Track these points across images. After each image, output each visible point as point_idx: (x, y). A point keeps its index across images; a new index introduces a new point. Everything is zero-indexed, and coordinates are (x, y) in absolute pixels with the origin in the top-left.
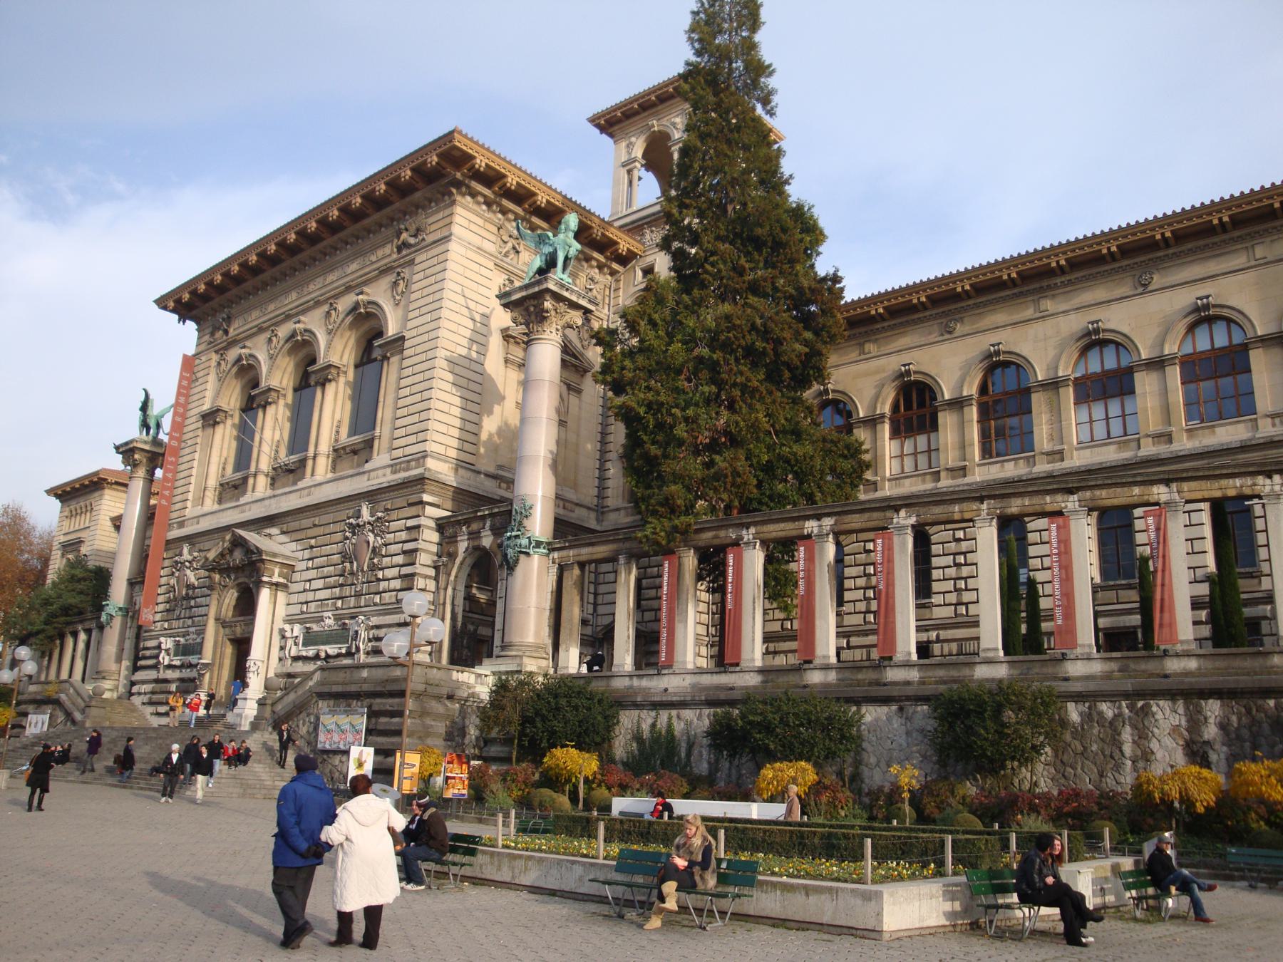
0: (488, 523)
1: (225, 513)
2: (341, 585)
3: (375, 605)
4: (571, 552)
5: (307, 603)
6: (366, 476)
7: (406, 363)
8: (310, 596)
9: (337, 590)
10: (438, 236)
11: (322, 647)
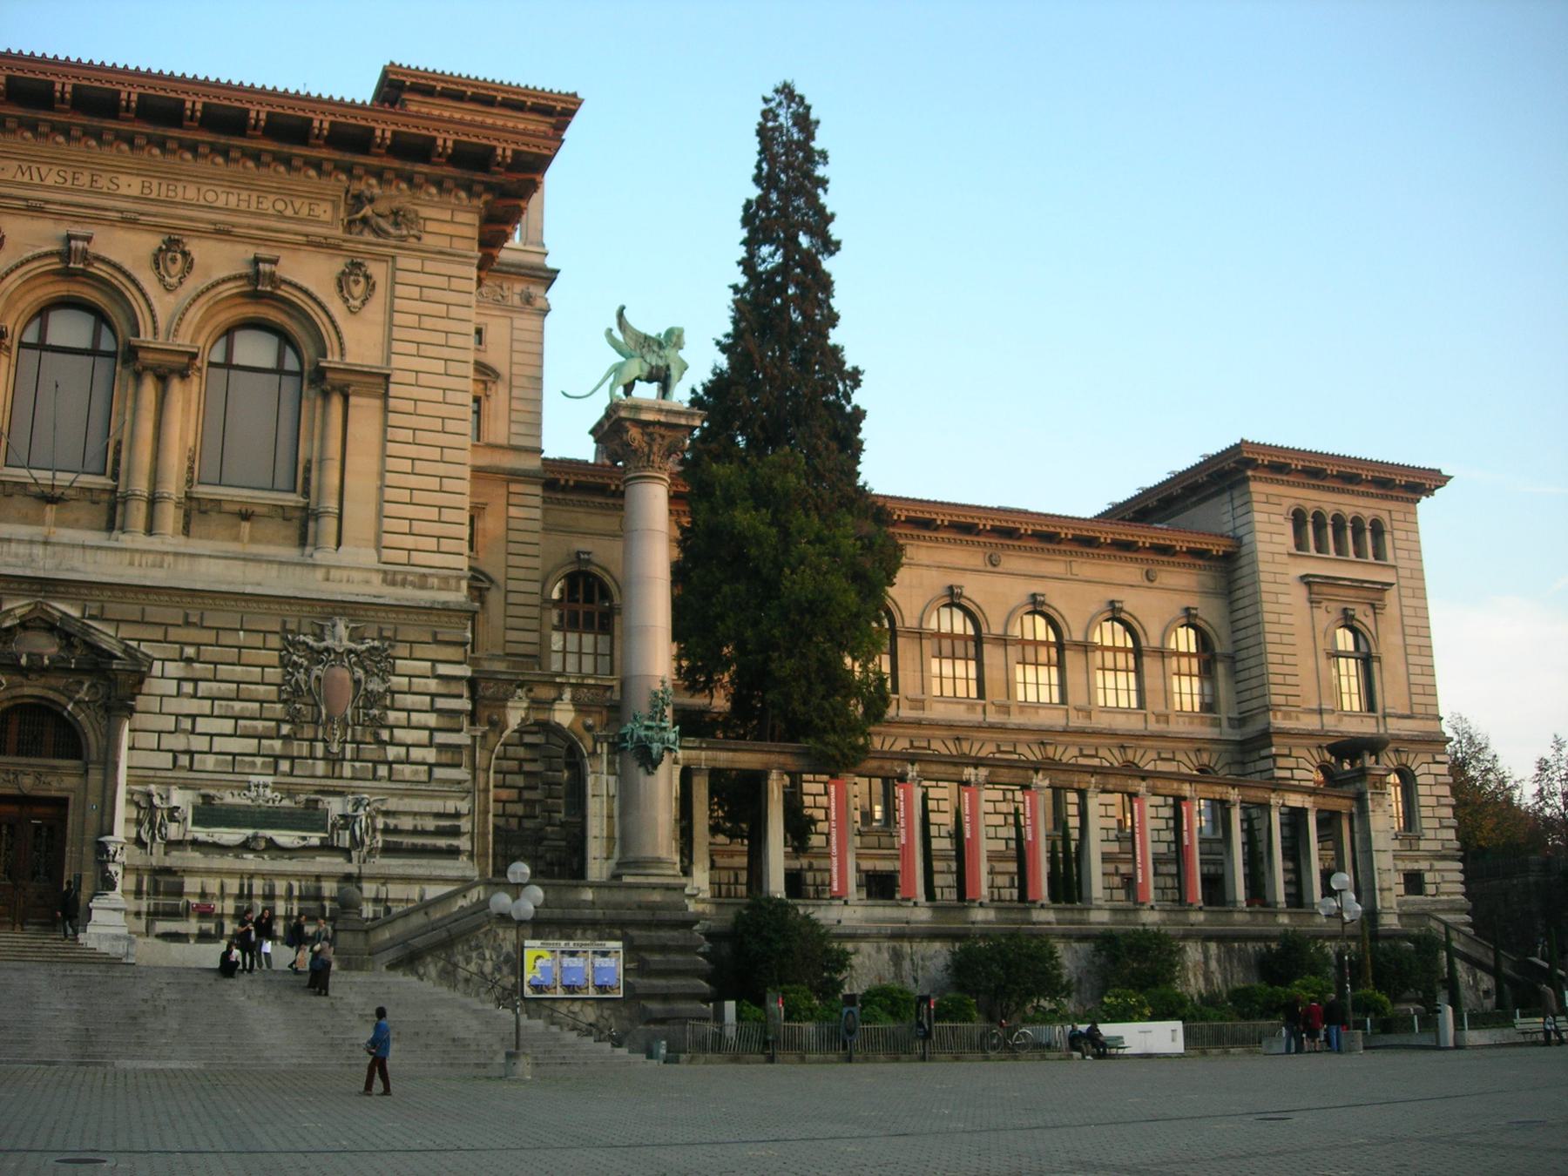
0: (567, 695)
2: (286, 738)
3: (375, 778)
4: (703, 754)
5: (191, 753)
6: (320, 574)
7: (394, 419)
8: (200, 743)
9: (277, 745)
10: (442, 243)
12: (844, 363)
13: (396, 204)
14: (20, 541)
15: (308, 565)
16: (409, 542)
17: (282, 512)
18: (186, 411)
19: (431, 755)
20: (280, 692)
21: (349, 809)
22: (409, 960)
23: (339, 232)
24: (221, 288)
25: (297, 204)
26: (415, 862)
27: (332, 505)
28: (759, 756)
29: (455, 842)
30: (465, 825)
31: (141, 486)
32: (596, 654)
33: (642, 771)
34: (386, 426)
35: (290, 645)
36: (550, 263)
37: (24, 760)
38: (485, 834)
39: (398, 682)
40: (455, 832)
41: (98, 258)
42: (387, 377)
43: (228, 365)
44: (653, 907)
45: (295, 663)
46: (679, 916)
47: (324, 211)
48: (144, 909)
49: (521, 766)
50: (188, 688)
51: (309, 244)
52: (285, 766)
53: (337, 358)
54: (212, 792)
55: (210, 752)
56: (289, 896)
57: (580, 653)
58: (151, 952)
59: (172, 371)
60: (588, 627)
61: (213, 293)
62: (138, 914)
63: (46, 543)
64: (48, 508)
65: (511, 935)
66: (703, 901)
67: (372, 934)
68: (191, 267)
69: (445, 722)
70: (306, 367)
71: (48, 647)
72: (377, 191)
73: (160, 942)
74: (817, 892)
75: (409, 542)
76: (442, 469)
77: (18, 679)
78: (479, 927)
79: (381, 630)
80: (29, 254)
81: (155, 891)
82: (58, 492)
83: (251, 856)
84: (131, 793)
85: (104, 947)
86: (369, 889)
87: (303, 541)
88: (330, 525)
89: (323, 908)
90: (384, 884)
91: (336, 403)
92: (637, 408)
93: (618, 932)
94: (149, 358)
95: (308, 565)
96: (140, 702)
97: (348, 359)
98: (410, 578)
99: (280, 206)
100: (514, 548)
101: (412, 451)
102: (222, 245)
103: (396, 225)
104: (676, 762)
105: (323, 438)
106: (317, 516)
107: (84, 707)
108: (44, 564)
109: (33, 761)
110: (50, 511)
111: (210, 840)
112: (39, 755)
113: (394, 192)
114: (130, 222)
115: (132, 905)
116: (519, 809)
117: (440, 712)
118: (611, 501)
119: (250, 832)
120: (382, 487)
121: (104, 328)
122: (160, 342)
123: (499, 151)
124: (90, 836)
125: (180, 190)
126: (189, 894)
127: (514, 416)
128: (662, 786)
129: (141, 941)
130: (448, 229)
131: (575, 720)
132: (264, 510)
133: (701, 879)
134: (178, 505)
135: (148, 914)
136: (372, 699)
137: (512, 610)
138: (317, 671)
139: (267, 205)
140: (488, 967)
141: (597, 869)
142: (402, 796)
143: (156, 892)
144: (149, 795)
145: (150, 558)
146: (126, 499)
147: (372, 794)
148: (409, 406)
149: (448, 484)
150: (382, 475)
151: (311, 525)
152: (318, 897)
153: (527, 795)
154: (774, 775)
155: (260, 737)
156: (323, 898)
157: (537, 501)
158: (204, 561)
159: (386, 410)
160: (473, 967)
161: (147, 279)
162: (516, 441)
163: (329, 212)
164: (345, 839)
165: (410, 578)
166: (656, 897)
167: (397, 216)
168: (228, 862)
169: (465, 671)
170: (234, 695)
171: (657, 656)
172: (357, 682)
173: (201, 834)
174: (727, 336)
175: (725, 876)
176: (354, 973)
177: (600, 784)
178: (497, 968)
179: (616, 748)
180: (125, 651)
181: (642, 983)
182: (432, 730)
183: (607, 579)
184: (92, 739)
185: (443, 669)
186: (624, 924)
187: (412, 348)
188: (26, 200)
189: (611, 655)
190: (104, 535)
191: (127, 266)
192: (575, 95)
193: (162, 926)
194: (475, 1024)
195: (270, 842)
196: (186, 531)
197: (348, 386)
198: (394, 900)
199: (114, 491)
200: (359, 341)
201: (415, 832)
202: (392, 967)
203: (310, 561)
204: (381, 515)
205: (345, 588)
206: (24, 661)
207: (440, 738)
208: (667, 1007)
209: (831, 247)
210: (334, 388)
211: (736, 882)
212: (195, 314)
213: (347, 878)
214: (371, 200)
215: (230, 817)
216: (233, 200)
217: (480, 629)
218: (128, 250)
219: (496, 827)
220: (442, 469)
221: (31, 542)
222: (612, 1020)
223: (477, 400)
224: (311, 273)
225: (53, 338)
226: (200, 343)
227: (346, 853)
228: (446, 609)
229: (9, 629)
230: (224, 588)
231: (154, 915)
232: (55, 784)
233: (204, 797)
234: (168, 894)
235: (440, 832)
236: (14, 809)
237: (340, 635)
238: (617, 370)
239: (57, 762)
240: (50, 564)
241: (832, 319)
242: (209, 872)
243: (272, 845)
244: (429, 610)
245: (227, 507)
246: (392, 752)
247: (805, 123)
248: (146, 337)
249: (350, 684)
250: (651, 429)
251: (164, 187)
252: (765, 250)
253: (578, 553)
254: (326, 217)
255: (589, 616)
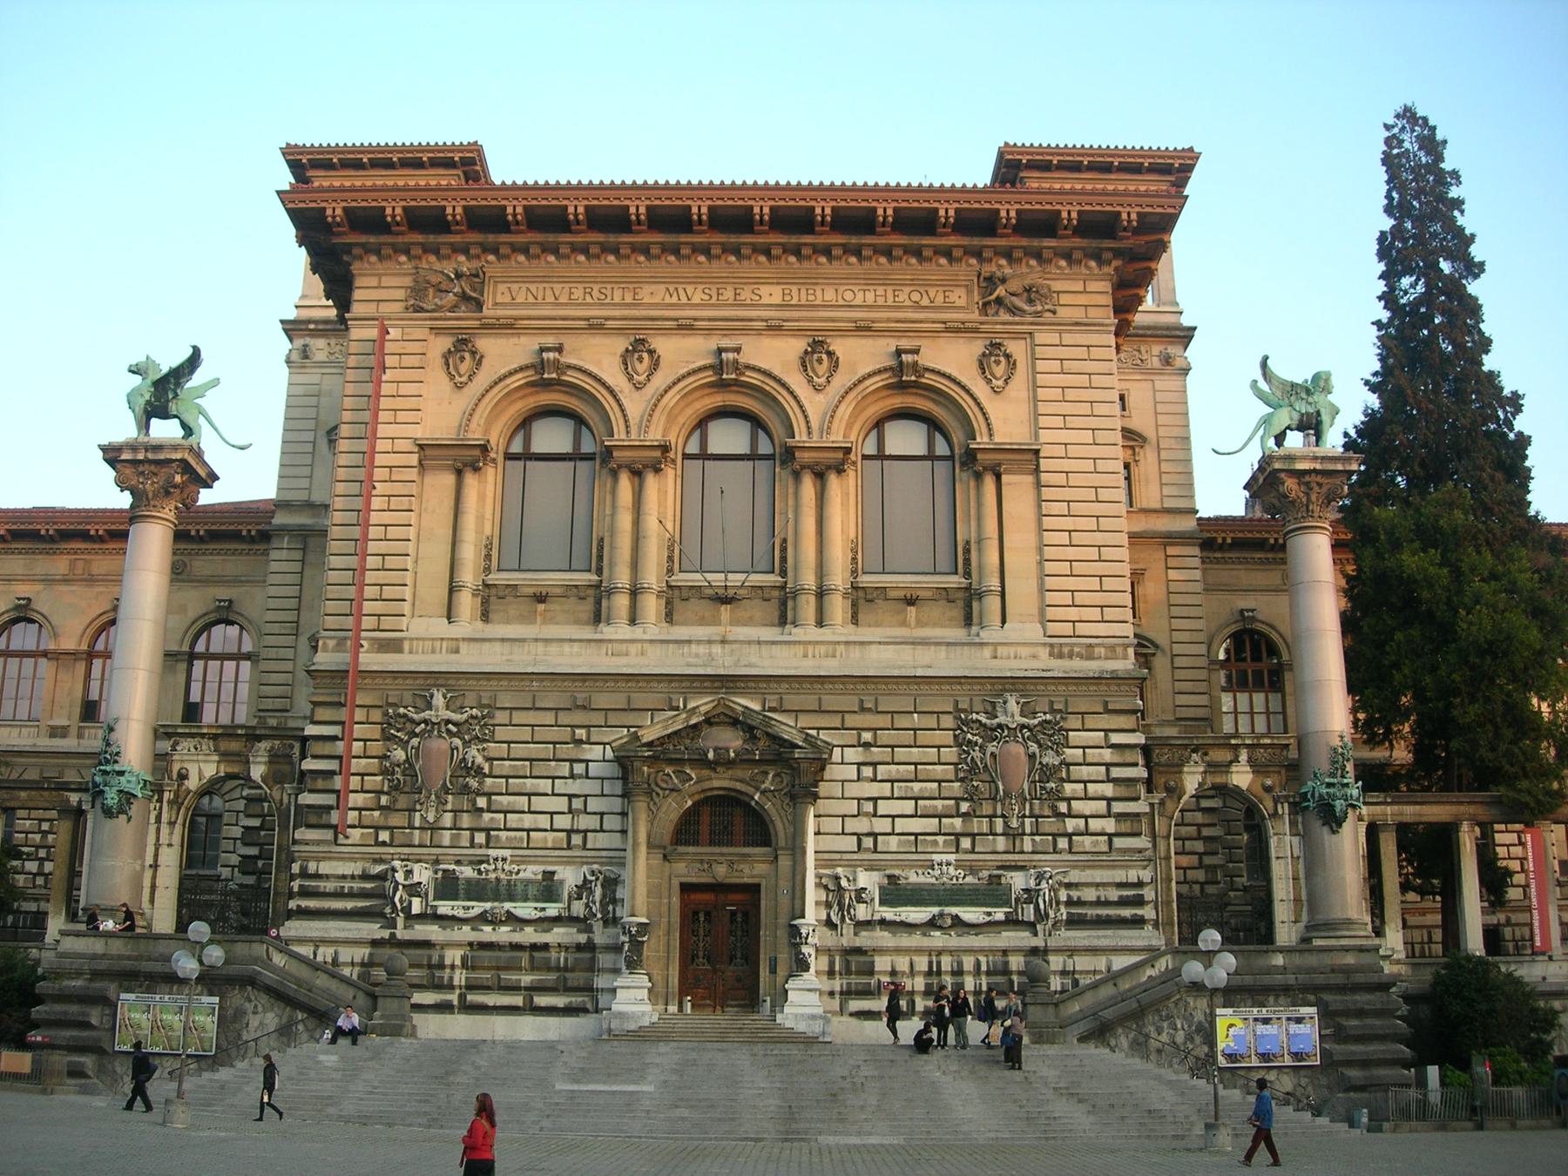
0: (1244, 757)
1: (553, 648)
3: (1055, 852)
4: (1389, 809)
5: (875, 835)
6: (987, 652)
7: (1047, 493)
8: (882, 825)
9: (957, 823)
10: (1078, 314)
11: (948, 910)
12: (1502, 389)
13: (1027, 282)
14: (699, 642)
15: (975, 644)
16: (1073, 613)
17: (945, 594)
18: (845, 504)
19: (1110, 825)
20: (957, 771)
21: (1032, 883)
22: (1100, 1032)
23: (975, 316)
24: (867, 383)
25: (932, 293)
26: (1101, 933)
27: (994, 583)
28: (1447, 807)
29: (1139, 912)
30: (1148, 893)
31: (809, 580)
32: (1267, 713)
33: (1326, 829)
34: (1040, 501)
35: (963, 724)
36: (1186, 321)
37: (717, 850)
38: (1169, 903)
39: (1073, 754)
40: (1139, 901)
41: (748, 367)
42: (1037, 452)
43: (881, 456)
44: (1347, 970)
45: (970, 741)
46: (1375, 978)
47: (958, 297)
48: (838, 989)
49: (1199, 832)
50: (867, 772)
51: (948, 330)
52: (966, 843)
53: (986, 439)
54: (897, 872)
55: (892, 834)
56: (977, 971)
57: (1252, 713)
58: (845, 1030)
59: (829, 468)
60: (1258, 685)
61: (861, 387)
62: (832, 994)
63: (723, 642)
64: (723, 608)
65: (1202, 1003)
66: (1398, 962)
67: (1061, 1006)
68: (836, 366)
69: (1122, 791)
70: (957, 451)
71: (732, 741)
72: (1008, 271)
73: (854, 1021)
74: (1516, 947)
75: (1073, 613)
76: (1099, 538)
77: (706, 773)
78: (1168, 997)
79: (1052, 703)
80: (684, 371)
81: (847, 971)
82: (731, 592)
83: (938, 933)
84: (819, 876)
85: (801, 1027)
86: (1056, 962)
87: (968, 621)
88: (993, 603)
89: (1012, 982)
90: (1070, 956)
91: (989, 483)
92: (1290, 458)
93: (1312, 998)
94: (803, 457)
95: (975, 644)
96: (823, 789)
97: (997, 439)
98: (1076, 650)
99: (915, 297)
100: (1176, 611)
101: (1068, 523)
102: (864, 341)
103: (1030, 301)
104: (1360, 819)
105: (979, 519)
106: (980, 596)
107: (770, 795)
108: (724, 662)
109: (725, 850)
110: (725, 611)
111: (898, 919)
112: (730, 844)
113: (1024, 269)
114: (775, 329)
115: (826, 984)
116: (1200, 875)
117: (1116, 781)
118: (1270, 555)
119: (935, 910)
120: (1041, 563)
121: (761, 433)
122: (815, 441)
123: (1124, 216)
124: (783, 920)
125: (819, 293)
126: (880, 972)
127: (1165, 478)
128: (1348, 843)
129: (835, 1020)
130: (1083, 300)
131: (1253, 781)
132: (929, 594)
133: (1394, 939)
134: (845, 595)
135: (842, 993)
136: (1048, 773)
137: (1179, 674)
138: (991, 748)
139: (903, 297)
140: (1180, 1037)
141: (1286, 932)
142: (1084, 868)
143: (848, 972)
144: (837, 878)
145: (823, 649)
146: (795, 594)
147: (1053, 867)
148: (1060, 479)
149: (1107, 553)
150: (1040, 551)
151: (975, 605)
152: (1006, 971)
153: (1208, 860)
154: (1465, 827)
155: (940, 817)
156: (1011, 973)
157: (1196, 562)
158: (873, 647)
159: (1039, 485)
160: (1164, 1038)
161: (797, 382)
162: (1169, 504)
163: (964, 296)
164: (1029, 913)
165: (1076, 650)
166: (1350, 959)
167: (1030, 293)
168: (916, 940)
169: (1138, 738)
170: (912, 776)
171: (1332, 710)
172: (1032, 757)
173: (889, 913)
174: (1375, 374)
175: (1417, 936)
176: (1045, 1046)
177: (1283, 845)
178: (1189, 1038)
179: (1297, 808)
180: (805, 740)
181: (1339, 1050)
182: (1109, 800)
183: (1274, 636)
184: (780, 827)
185: (1116, 738)
186: (1316, 989)
187: (1059, 422)
188: (676, 320)
189: (1284, 712)
190: (777, 630)
191: (776, 372)
192: (1191, 149)
193: (856, 1005)
194: (1170, 1096)
195: (956, 918)
196: (855, 620)
197: (999, 465)
198: (1081, 972)
199: (783, 587)
200: (1005, 419)
201: (1099, 903)
202: (1083, 1039)
203: (977, 640)
204: (1043, 590)
205: (1015, 664)
206: (711, 755)
207: (1118, 807)
208: (1366, 1073)
209: (1475, 269)
210: (985, 469)
211: (1430, 941)
212: (845, 410)
213: (1034, 951)
214: (1003, 281)
215: (916, 896)
216: (870, 297)
217: (1148, 695)
218: (775, 355)
219: (1179, 895)
220: (1099, 538)
221: (710, 642)
222: (1310, 1088)
223: (1127, 466)
224: (953, 358)
225: (712, 450)
226: (853, 438)
227: (1031, 926)
228: (1115, 678)
229: (695, 726)
230: (896, 673)
231: (847, 994)
232: (747, 871)
233: (889, 877)
234: (859, 973)
235: (1123, 902)
236: (709, 897)
237: (1012, 711)
238: (1266, 421)
239: (746, 850)
240: (729, 661)
241: (1485, 344)
242: (898, 951)
243: (958, 922)
244: (1098, 679)
245: (892, 594)
246: (1071, 824)
247: (1432, 145)
248: (801, 437)
249: (1024, 759)
250: (1307, 478)
251: (803, 292)
252: (1406, 282)
253: (1242, 611)
254: (962, 302)
255: (1258, 675)
